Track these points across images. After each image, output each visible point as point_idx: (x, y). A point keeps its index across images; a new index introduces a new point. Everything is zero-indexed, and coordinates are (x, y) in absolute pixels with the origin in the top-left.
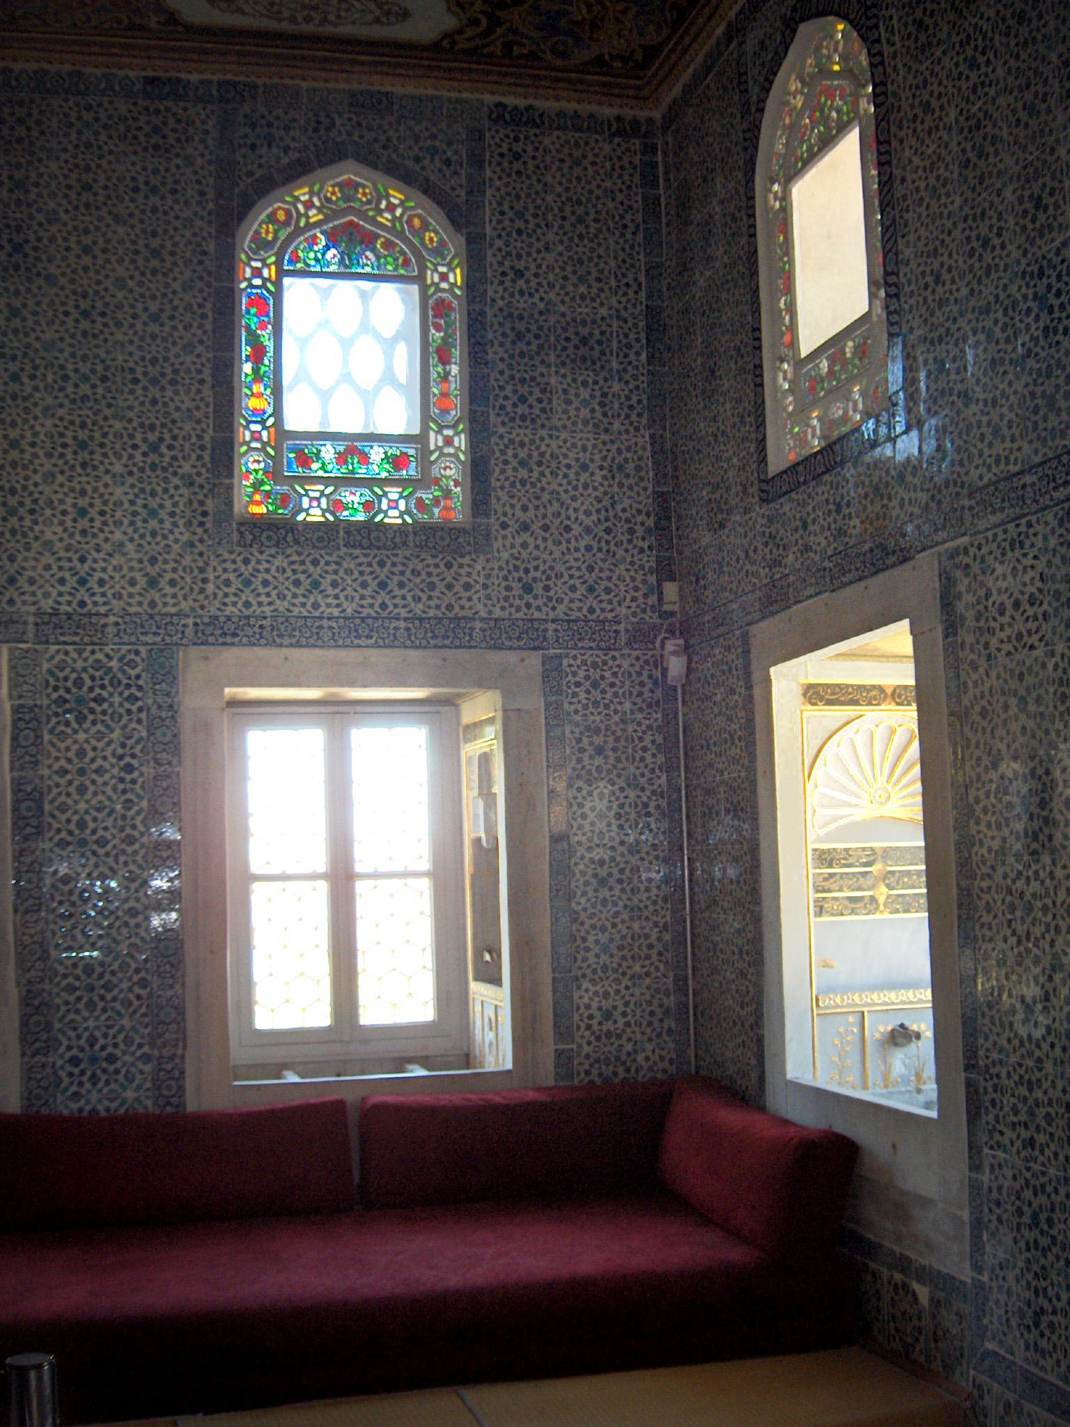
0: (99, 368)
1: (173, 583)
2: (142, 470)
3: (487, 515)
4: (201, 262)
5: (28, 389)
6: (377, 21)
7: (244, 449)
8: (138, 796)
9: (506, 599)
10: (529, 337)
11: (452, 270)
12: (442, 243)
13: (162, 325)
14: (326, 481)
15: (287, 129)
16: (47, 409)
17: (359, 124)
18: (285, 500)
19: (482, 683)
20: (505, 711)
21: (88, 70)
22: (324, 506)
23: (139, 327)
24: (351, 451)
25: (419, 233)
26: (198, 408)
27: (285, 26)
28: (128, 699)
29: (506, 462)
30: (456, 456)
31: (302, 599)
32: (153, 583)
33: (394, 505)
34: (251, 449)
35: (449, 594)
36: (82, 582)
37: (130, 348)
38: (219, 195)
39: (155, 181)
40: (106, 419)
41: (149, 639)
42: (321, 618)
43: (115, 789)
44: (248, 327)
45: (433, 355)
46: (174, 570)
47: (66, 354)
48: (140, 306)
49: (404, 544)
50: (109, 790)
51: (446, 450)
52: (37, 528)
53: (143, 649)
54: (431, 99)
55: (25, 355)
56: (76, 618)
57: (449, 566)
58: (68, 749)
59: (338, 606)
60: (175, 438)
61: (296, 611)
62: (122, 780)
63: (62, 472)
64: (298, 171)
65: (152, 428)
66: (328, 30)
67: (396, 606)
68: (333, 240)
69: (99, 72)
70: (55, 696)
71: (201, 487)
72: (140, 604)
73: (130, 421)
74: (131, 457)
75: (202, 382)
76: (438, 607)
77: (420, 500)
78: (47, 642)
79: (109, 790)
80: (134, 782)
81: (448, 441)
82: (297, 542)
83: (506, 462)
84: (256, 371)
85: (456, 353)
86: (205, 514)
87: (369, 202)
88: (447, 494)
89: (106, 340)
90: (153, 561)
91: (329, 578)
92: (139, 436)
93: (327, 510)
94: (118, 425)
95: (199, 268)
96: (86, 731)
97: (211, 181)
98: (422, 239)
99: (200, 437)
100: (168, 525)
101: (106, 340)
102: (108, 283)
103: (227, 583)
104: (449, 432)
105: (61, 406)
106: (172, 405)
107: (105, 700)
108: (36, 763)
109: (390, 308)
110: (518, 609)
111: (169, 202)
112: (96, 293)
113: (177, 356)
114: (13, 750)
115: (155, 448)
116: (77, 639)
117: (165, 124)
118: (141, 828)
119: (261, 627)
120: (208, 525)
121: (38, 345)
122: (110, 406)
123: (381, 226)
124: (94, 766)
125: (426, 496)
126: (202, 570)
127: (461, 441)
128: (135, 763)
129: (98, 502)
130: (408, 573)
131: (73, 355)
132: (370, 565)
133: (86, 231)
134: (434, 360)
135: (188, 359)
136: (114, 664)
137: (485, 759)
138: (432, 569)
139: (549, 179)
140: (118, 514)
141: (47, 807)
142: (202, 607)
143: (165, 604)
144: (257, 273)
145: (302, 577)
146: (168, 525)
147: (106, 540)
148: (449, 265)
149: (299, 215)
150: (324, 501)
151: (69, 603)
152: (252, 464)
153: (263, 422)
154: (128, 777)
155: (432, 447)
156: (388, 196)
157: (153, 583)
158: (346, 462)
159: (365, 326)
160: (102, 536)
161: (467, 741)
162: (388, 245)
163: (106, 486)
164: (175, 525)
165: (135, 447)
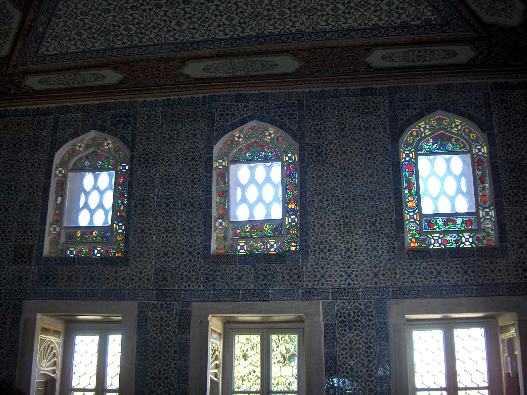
0: (351, 195)
1: (383, 275)
2: (369, 232)
3: (506, 242)
4: (386, 154)
5: (326, 205)
6: (445, 57)
7: (407, 222)
8: (373, 358)
9: (516, 275)
10: (516, 170)
11: (483, 147)
12: (478, 137)
13: (374, 178)
14: (440, 233)
15: (414, 101)
16: (333, 212)
17: (441, 96)
18: (424, 241)
19: (509, 310)
20: (519, 321)
21: (340, 88)
22: (440, 242)
23: (365, 179)
24: (449, 220)
25: (468, 134)
26: (389, 208)
27: (411, 64)
28: (368, 320)
29: (511, 220)
30: (490, 219)
31: (434, 279)
32: (376, 275)
33: (467, 240)
34: (410, 222)
35: (493, 274)
36: (349, 276)
37: (362, 187)
38: (391, 128)
39: (367, 125)
40: (355, 214)
41: (375, 297)
42: (442, 286)
43: (364, 356)
44: (406, 176)
45: (478, 181)
46: (384, 270)
47: (339, 191)
48: (365, 172)
49: (473, 255)
50: (362, 356)
51: (487, 217)
52: (331, 256)
53: (373, 301)
54: (467, 84)
55: (324, 193)
56: (347, 290)
57: (492, 263)
58: (346, 340)
59: (448, 281)
60: (381, 220)
61: (432, 284)
62: (367, 352)
63: (340, 235)
64: (420, 116)
65: (372, 216)
66: (427, 63)
67: (471, 280)
68: (435, 140)
69: (344, 89)
70: (340, 320)
71: (392, 238)
72: (371, 283)
73: (364, 214)
74: (365, 228)
75: (390, 198)
76: (488, 280)
77: (478, 238)
78: (337, 299)
79: (362, 356)
80: (371, 353)
81: (487, 214)
82: (430, 257)
83: (511, 220)
84: (410, 192)
85: (487, 179)
86: (394, 248)
87: (448, 125)
88: (489, 234)
89: (353, 185)
90: (375, 267)
91: (444, 270)
92: (368, 220)
93: (441, 244)
94: (360, 216)
95: (386, 156)
96: (352, 333)
97: (388, 123)
98: (470, 137)
99: (391, 219)
100: (380, 253)
101: (353, 185)
102: (353, 164)
103: (404, 274)
104: (488, 210)
105: (338, 210)
106: (379, 207)
107: (359, 321)
108: (334, 346)
109: (458, 163)
110: (521, 279)
111: (373, 132)
112: (348, 168)
113: (380, 189)
114: (325, 341)
115: (374, 224)
116: (348, 298)
117: (369, 104)
118: (375, 371)
119: (419, 291)
120: (396, 252)
121: (328, 189)
122: (356, 209)
123: (453, 133)
124: (356, 347)
125: (480, 236)
126: (394, 270)
127: (492, 213)
128: (372, 345)
129: (353, 245)
130: (475, 267)
131: (342, 191)
132: (460, 264)
133: (343, 146)
134: (478, 182)
135: (384, 190)
136: (362, 307)
137: (510, 341)
138: (485, 265)
139: (517, 108)
140: (361, 250)
141: (338, 363)
142: (395, 284)
143: (381, 283)
144: (407, 155)
145: (433, 270)
146: (380, 253)
147: (357, 260)
148: (481, 145)
149: (422, 133)
150: (440, 240)
151: (344, 284)
152: (411, 227)
153: (414, 211)
154: (369, 351)
155: (481, 216)
156: (455, 122)
157: (376, 275)
158: (447, 225)
159: (449, 171)
160: (356, 258)
161: (501, 333)
162: (457, 140)
163: (356, 239)
164: (383, 252)
165: (366, 224)
